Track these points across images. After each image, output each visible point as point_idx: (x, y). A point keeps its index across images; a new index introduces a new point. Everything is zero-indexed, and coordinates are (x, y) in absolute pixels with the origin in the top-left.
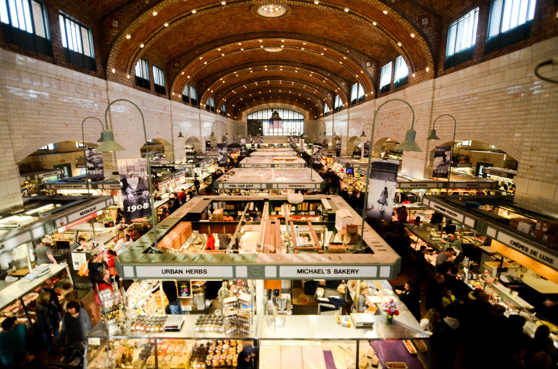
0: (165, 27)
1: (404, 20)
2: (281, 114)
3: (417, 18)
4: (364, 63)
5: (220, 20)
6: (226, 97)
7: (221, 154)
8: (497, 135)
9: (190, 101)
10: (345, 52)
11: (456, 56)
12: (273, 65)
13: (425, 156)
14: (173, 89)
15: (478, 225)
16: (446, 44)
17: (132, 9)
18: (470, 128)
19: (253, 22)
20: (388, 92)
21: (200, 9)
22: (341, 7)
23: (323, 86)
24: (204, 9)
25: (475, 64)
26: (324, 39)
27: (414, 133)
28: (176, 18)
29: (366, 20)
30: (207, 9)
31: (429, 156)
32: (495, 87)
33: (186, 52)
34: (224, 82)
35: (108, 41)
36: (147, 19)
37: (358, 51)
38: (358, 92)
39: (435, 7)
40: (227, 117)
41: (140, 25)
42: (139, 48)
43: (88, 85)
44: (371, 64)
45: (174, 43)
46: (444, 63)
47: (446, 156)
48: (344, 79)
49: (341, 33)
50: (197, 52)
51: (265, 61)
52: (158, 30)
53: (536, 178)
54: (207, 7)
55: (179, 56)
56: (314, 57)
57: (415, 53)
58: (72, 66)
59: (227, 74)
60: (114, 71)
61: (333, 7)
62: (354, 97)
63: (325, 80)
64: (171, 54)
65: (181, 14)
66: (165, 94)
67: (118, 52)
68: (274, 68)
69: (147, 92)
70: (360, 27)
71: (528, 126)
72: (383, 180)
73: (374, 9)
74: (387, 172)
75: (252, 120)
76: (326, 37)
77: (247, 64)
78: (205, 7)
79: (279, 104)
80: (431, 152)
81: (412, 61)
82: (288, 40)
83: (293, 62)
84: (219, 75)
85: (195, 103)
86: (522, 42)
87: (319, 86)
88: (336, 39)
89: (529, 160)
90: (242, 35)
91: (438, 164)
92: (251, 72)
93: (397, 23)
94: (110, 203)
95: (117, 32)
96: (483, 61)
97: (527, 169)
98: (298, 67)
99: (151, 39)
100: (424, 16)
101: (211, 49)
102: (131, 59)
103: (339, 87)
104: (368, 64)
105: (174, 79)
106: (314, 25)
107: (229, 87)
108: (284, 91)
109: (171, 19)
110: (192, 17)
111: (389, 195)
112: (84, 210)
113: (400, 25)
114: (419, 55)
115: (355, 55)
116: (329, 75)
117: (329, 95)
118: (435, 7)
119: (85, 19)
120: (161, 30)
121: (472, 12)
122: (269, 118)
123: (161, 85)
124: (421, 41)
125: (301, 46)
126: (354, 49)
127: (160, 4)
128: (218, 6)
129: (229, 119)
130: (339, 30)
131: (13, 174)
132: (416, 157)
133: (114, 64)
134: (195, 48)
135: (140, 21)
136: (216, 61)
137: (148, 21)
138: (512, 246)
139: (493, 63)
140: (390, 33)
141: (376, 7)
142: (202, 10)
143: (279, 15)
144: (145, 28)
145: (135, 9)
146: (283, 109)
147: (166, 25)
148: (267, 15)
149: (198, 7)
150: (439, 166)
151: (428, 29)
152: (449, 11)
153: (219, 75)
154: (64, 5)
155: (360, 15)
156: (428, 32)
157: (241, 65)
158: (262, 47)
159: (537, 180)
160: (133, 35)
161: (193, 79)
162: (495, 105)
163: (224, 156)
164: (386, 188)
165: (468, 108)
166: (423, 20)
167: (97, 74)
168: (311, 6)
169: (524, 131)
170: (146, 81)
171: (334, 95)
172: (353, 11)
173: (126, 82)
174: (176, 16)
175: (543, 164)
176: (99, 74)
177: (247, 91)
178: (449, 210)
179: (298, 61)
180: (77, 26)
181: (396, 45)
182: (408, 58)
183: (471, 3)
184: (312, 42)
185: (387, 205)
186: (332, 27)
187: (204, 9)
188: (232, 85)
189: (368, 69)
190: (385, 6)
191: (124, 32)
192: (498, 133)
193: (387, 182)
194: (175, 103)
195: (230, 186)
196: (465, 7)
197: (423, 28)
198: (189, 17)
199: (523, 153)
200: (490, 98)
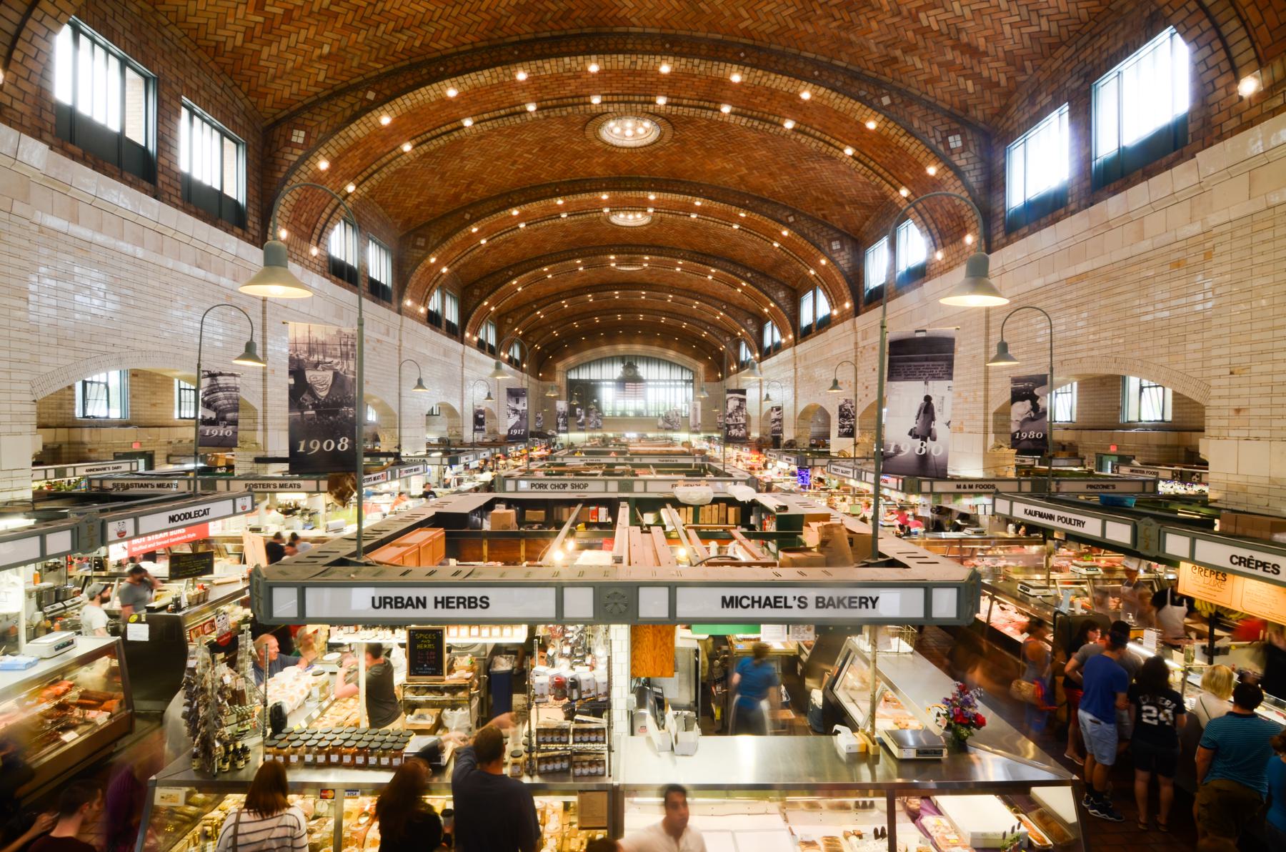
0: (404, 153)
1: (912, 140)
3: (938, 134)
4: (826, 243)
5: (519, 150)
6: (522, 324)
7: (516, 412)
8: (1146, 353)
9: (444, 325)
10: (784, 219)
12: (629, 253)
13: (982, 423)
14: (408, 292)
15: (1139, 535)
16: (1004, 184)
17: (338, 109)
18: (1079, 347)
19: (589, 157)
21: (481, 117)
22: (776, 119)
23: (736, 302)
24: (490, 120)
25: (1073, 213)
26: (739, 193)
28: (429, 135)
29: (830, 145)
30: (496, 118)
31: (991, 424)
32: (1126, 253)
33: (444, 216)
34: (520, 289)
35: (280, 171)
36: (367, 132)
37: (813, 219)
38: (814, 307)
39: (973, 113)
40: (522, 370)
41: (351, 143)
42: (343, 193)
43: (224, 255)
44: (842, 245)
45: (418, 196)
46: (1004, 223)
47: (1037, 397)
48: (782, 283)
49: (775, 180)
50: (467, 216)
51: (611, 246)
52: (389, 156)
53: (1253, 434)
54: (497, 114)
55: (428, 224)
56: (717, 237)
57: (938, 207)
58: (193, 210)
59: (526, 271)
60: (283, 234)
61: (761, 120)
62: (806, 318)
63: (741, 287)
64: (410, 220)
65: (439, 127)
66: (390, 301)
67: (296, 197)
69: (351, 290)
70: (817, 166)
72: (919, 379)
73: (848, 121)
74: (927, 360)
75: (578, 381)
76: (743, 189)
77: (572, 250)
78: (492, 115)
79: (638, 348)
80: (995, 414)
81: (933, 226)
83: (672, 248)
84: (510, 273)
85: (454, 332)
86: (1172, 155)
87: (726, 303)
88: (766, 195)
89: (1229, 397)
91: (1020, 419)
92: (581, 269)
93: (897, 147)
94: (244, 508)
95: (300, 152)
96: (1092, 205)
97: (1229, 418)
98: (682, 258)
99: (371, 175)
100: (953, 132)
101: (496, 211)
102: (324, 216)
104: (836, 246)
105: (412, 271)
106: (719, 163)
107: (529, 304)
108: (651, 318)
109: (419, 136)
110: (463, 134)
111: (937, 415)
112: (179, 512)
113: (903, 151)
114: (948, 212)
115: (807, 227)
116: (749, 275)
117: (750, 322)
118: (973, 113)
119: (233, 121)
120: (394, 158)
121: (1054, 115)
122: (615, 378)
123: (383, 282)
124: (952, 180)
125: (689, 208)
126: (804, 215)
127: (399, 100)
128: (519, 113)
129: (526, 376)
131: (21, 423)
133: (286, 220)
134: (464, 209)
135: (351, 134)
136: (506, 241)
137: (369, 136)
138: (1237, 568)
139: (1113, 205)
140: (881, 171)
141: (852, 115)
142: (485, 121)
143: (645, 142)
144: (361, 150)
145: (344, 109)
146: (649, 360)
147: (407, 147)
148: (619, 143)
149: (476, 115)
150: (1023, 423)
151: (963, 156)
152: (1004, 120)
153: (510, 273)
154: (194, 87)
155: (818, 134)
156: (963, 162)
157: (559, 253)
158: (606, 210)
159: (1258, 439)
160: (334, 162)
161: (455, 274)
162: (1131, 291)
163: (521, 418)
164: (928, 399)
165: (1070, 307)
166: (951, 139)
167: (246, 235)
168: (715, 117)
169: (1206, 335)
170: (351, 269)
171: (760, 321)
172: (803, 127)
173: (307, 263)
174: (429, 131)
175: (1266, 401)
176: (251, 237)
177: (570, 317)
178: (1062, 514)
179: (683, 247)
180: (216, 134)
181: (895, 194)
182: (923, 220)
183: (1050, 98)
184: (714, 199)
185: (934, 439)
186: (756, 168)
187: (490, 120)
188: (537, 301)
189: (835, 255)
190: (869, 111)
191: (316, 154)
192: (1147, 348)
193: (930, 383)
194: (409, 322)
196: (1038, 107)
197: (952, 154)
198: (456, 134)
199: (1214, 382)
200: (1116, 278)
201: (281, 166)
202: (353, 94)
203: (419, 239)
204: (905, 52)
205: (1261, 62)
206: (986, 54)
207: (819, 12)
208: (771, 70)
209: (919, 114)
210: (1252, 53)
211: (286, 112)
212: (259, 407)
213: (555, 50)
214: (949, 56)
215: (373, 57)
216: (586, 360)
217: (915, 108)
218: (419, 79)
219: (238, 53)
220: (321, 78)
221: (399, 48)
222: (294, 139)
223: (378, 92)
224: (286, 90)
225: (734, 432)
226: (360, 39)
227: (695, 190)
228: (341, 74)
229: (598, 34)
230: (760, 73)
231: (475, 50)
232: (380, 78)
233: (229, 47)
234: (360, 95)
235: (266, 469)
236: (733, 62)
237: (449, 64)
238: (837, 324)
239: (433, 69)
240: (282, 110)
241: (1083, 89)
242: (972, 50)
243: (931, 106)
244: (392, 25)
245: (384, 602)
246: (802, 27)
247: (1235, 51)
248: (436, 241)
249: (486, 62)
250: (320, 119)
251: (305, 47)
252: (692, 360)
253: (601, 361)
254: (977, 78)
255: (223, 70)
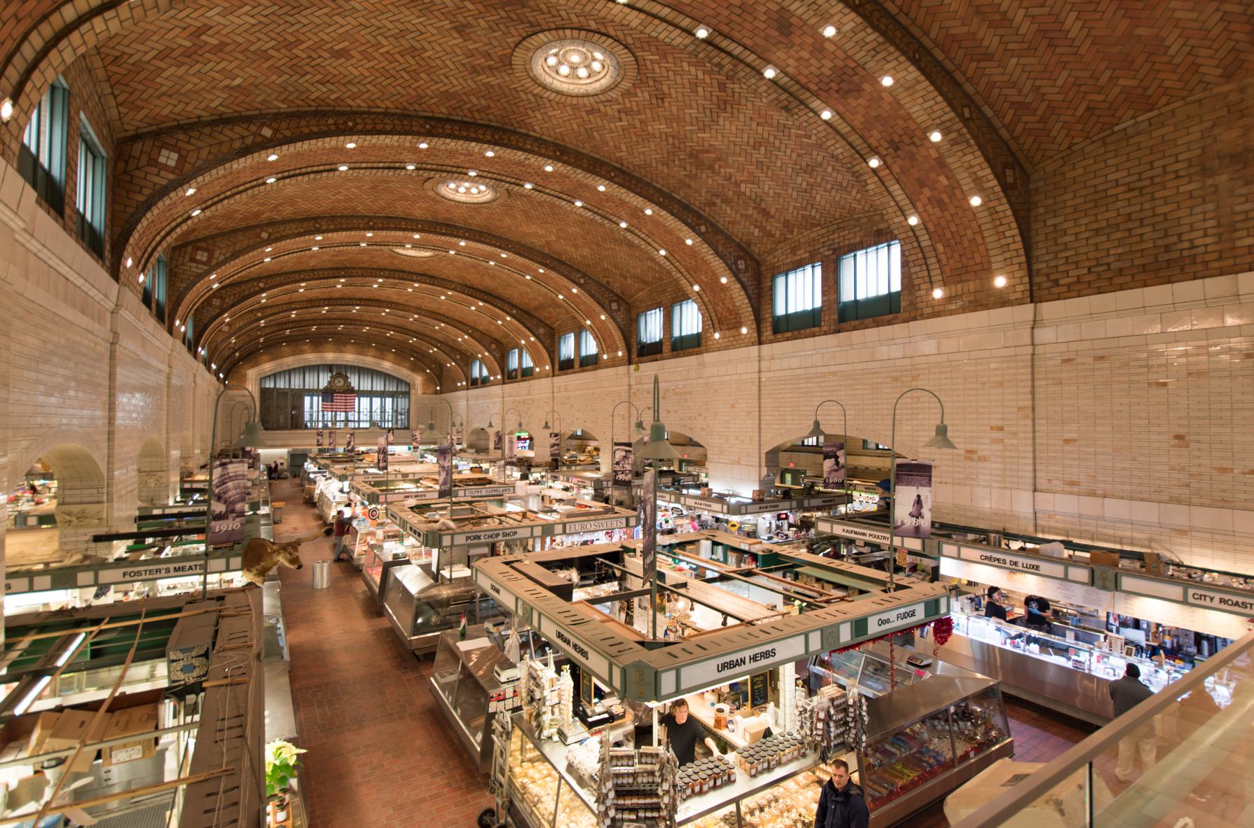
2: (354, 381)
11: (787, 317)
17: (222, 138)
20: (658, 356)
23: (481, 328)
25: (826, 333)
27: (945, 427)
31: (763, 461)
33: (234, 231)
35: (140, 193)
39: (753, 247)
50: (265, 235)
51: (381, 270)
55: (213, 237)
61: (603, 216)
63: (503, 320)
68: (394, 286)
71: (920, 416)
76: (546, 250)
77: (337, 269)
79: (349, 357)
82: (472, 244)
84: (262, 285)
88: (564, 258)
90: (379, 218)
95: (171, 176)
100: (740, 258)
101: (300, 235)
102: (158, 238)
103: (535, 335)
104: (614, 306)
117: (493, 346)
121: (809, 268)
125: (489, 257)
130: (575, 246)
132: (739, 463)
142: (360, 168)
145: (232, 140)
146: (361, 371)
148: (451, 196)
150: (830, 473)
153: (262, 285)
195: (468, 538)
201: (141, 188)
202: (245, 126)
203: (199, 252)
204: (723, 201)
205: (945, 283)
206: (773, 217)
207: (677, 162)
208: (633, 191)
209: (722, 242)
210: (940, 277)
211: (154, 128)
212: (105, 474)
213: (465, 134)
214: (750, 212)
215: (281, 98)
216: (286, 368)
217: (719, 237)
218: (325, 129)
219: (138, 67)
220: (213, 105)
221: (313, 96)
222: (162, 160)
223: (276, 131)
224: (166, 109)
225: (621, 477)
226: (278, 81)
227: (505, 244)
228: (238, 105)
229: (504, 130)
230: (623, 190)
231: (386, 114)
232: (278, 116)
233: (132, 60)
234: (253, 128)
235: (111, 547)
236: (602, 176)
237: (358, 120)
238: (607, 367)
239: (341, 121)
240: (150, 125)
241: (834, 257)
242: (766, 213)
243: (728, 238)
244: (320, 77)
245: (725, 666)
246: (660, 167)
247: (932, 273)
248: (222, 258)
249: (398, 128)
250: (199, 143)
251: (217, 75)
252: (410, 373)
253: (303, 370)
254: (762, 228)
255: (108, 79)
